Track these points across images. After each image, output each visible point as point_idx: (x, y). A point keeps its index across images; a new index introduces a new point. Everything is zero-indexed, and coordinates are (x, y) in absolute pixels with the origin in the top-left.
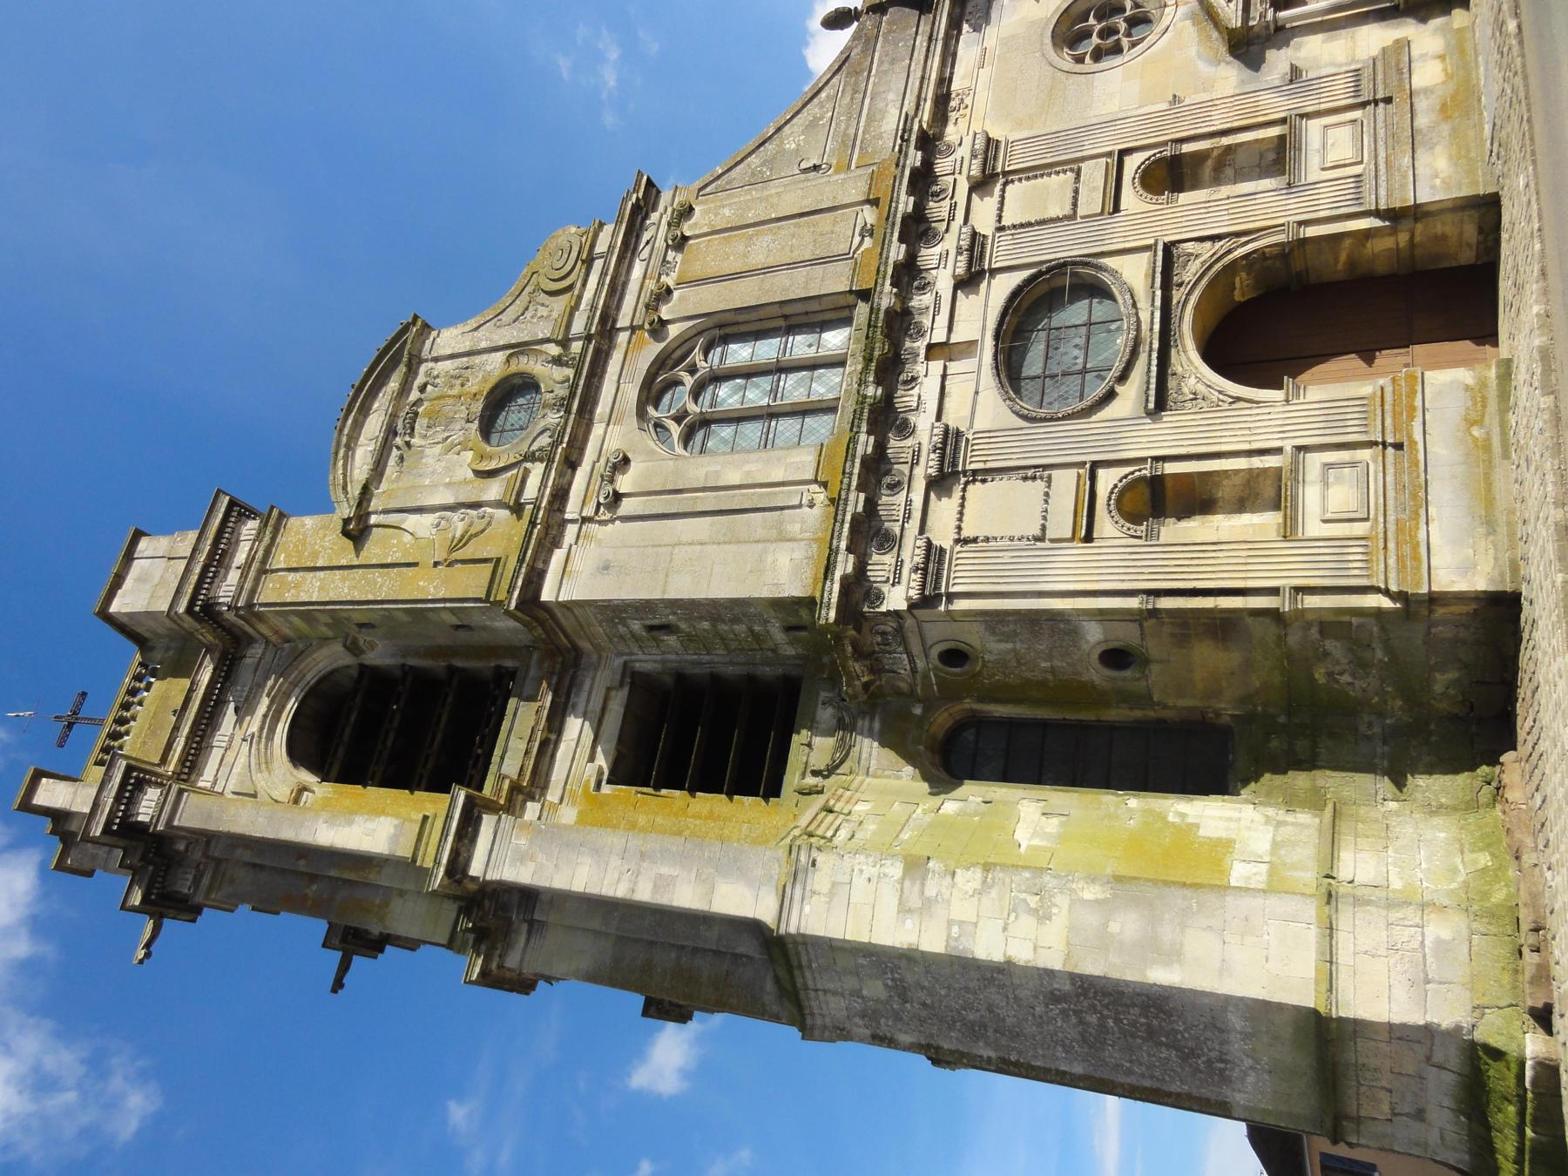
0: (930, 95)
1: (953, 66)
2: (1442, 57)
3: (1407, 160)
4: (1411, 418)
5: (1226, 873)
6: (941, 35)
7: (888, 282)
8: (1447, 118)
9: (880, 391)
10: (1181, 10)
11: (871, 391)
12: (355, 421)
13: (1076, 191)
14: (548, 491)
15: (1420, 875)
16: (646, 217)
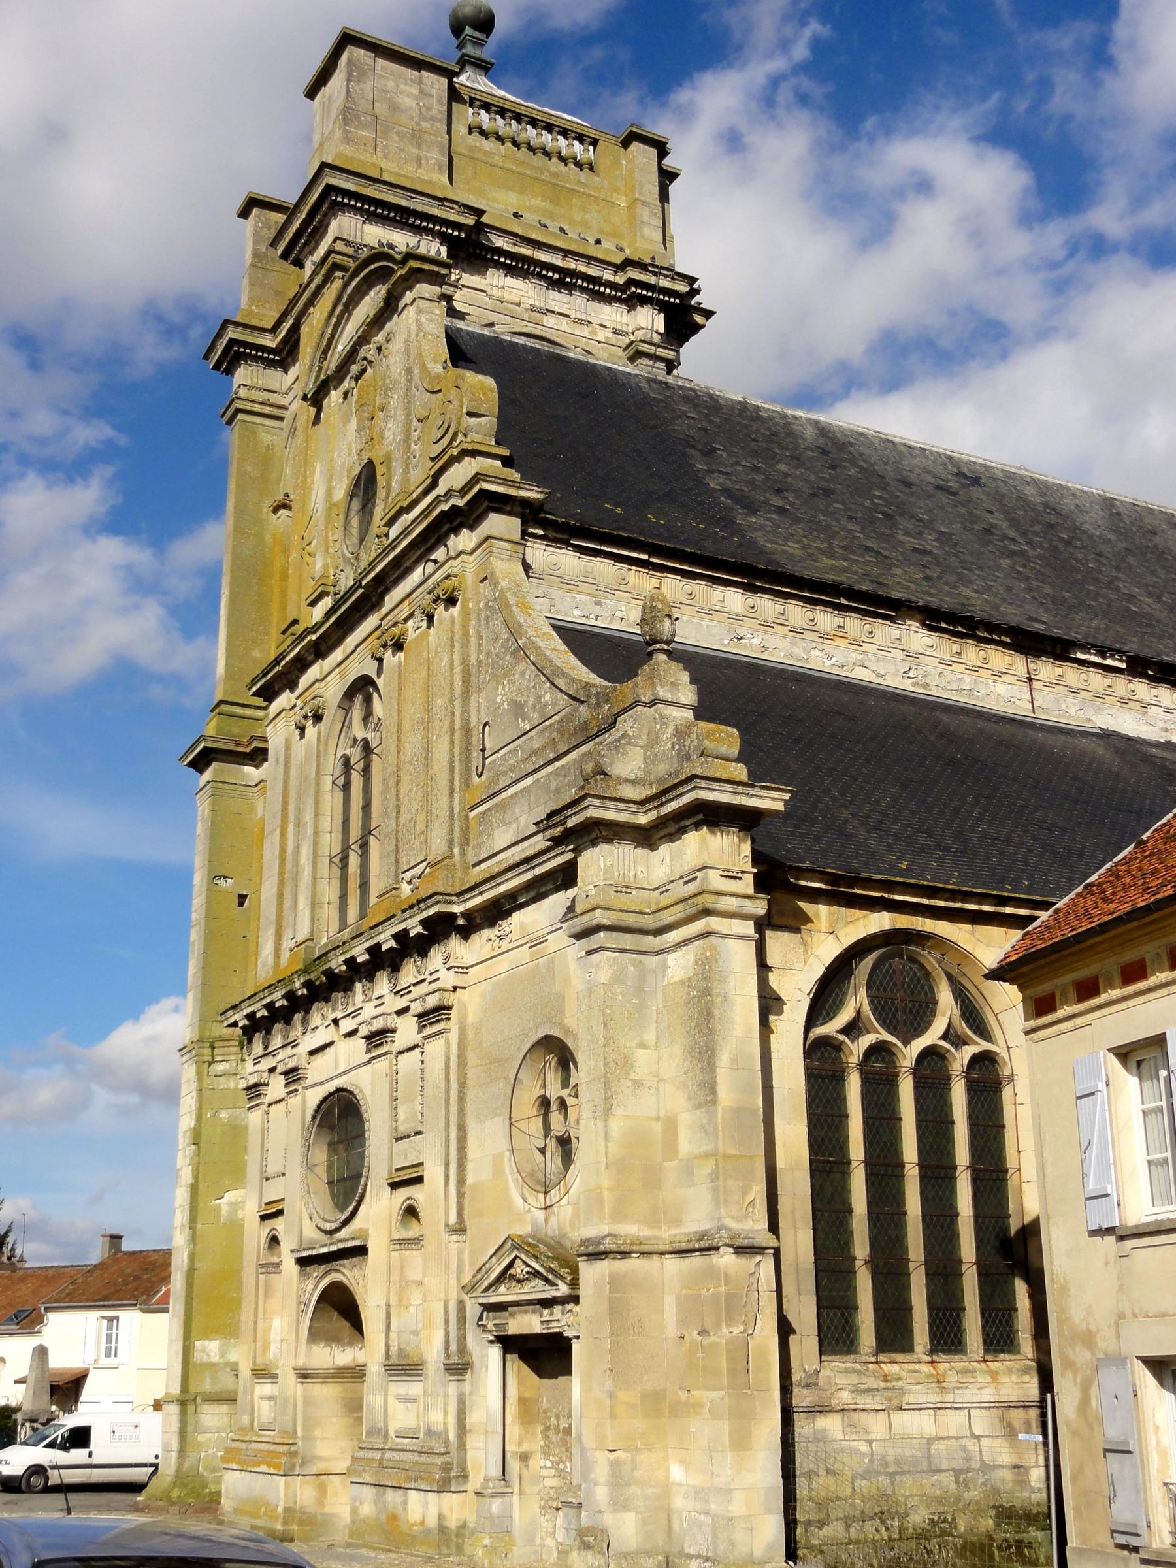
0: (488, 896)
1: (535, 900)
2: (423, 1523)
3: (367, 1479)
4: (269, 1466)
5: (207, 1335)
6: (539, 871)
7: (342, 958)
8: (388, 1518)
9: (300, 993)
10: (541, 1214)
11: (298, 984)
12: (358, 287)
13: (409, 1136)
14: (292, 655)
15: (210, 1451)
16: (456, 531)
